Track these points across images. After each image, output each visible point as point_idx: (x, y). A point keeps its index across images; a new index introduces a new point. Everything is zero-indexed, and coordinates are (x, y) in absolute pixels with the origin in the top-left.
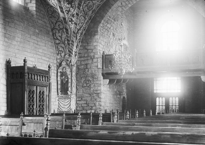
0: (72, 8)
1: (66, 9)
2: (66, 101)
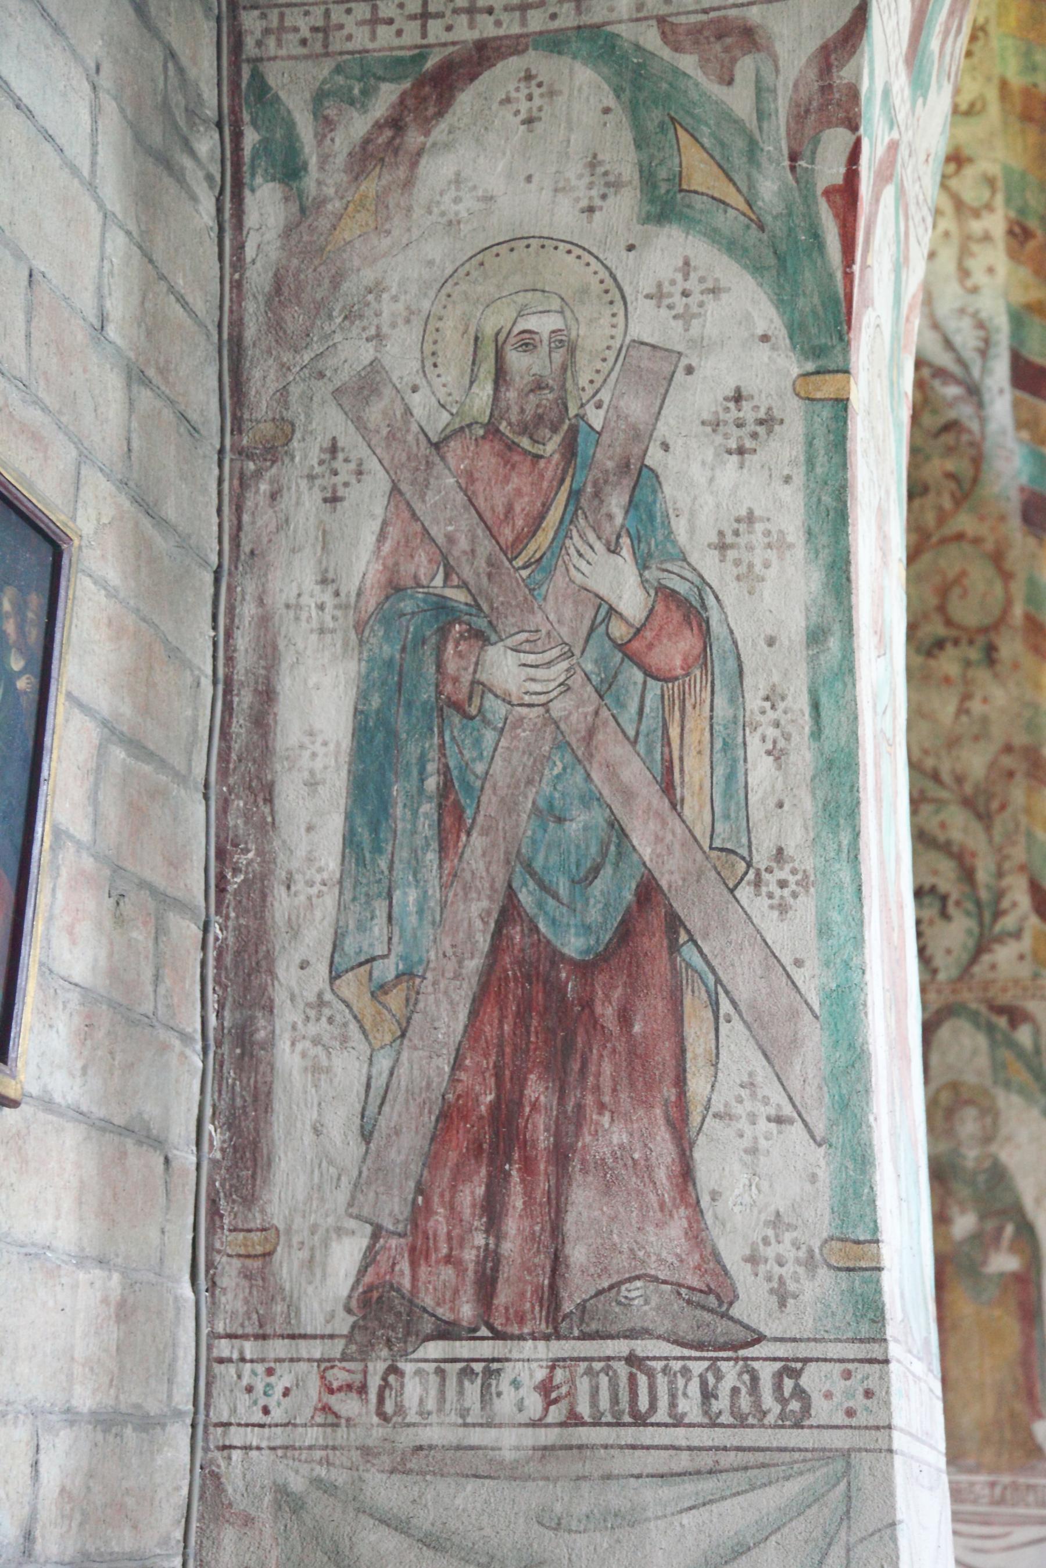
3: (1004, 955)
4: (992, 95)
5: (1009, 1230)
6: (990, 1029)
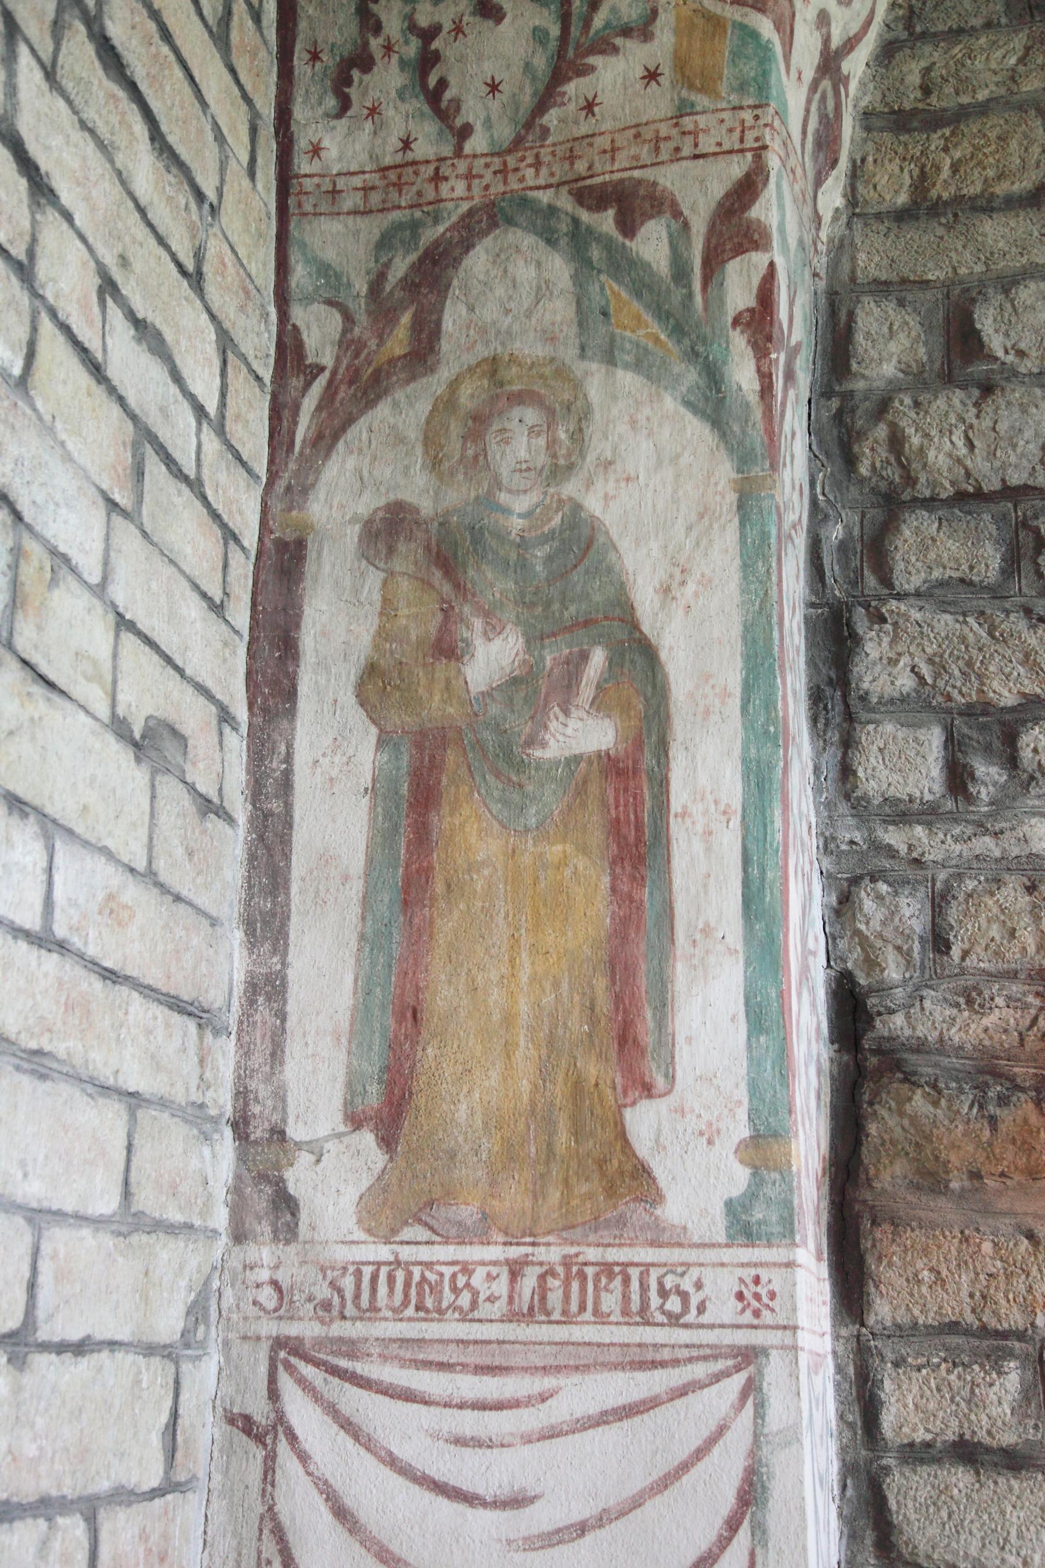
3: (613, 77)
5: (598, 658)
6: (579, 239)
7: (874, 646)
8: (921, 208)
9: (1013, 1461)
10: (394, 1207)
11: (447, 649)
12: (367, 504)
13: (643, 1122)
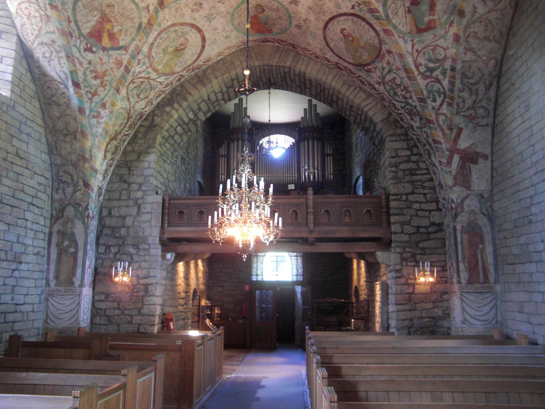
0: (102, 89)
1: (88, 89)
2: (68, 302)
3: (78, 194)
4: (56, 30)
5: (74, 244)
6: (75, 208)
7: (101, 240)
8: (109, 200)
9: (103, 301)
10: (56, 285)
11: (63, 242)
12: (57, 229)
13: (74, 279)
